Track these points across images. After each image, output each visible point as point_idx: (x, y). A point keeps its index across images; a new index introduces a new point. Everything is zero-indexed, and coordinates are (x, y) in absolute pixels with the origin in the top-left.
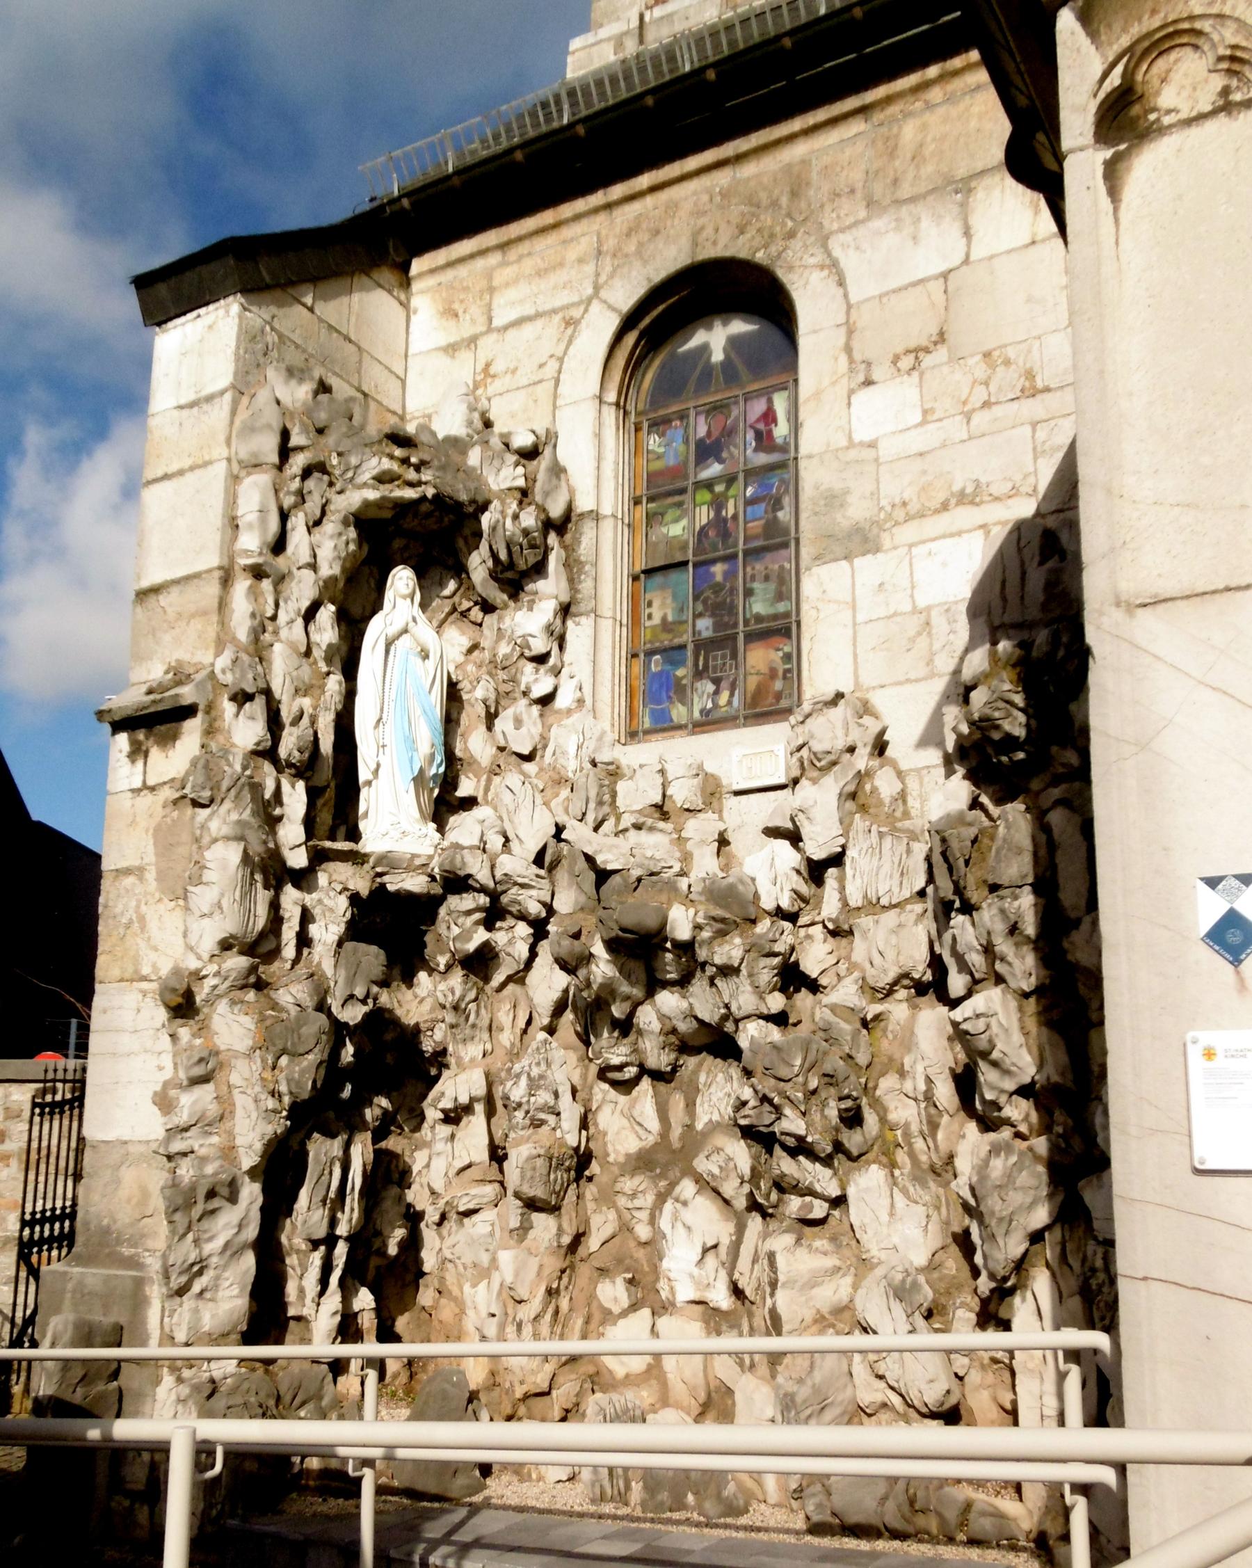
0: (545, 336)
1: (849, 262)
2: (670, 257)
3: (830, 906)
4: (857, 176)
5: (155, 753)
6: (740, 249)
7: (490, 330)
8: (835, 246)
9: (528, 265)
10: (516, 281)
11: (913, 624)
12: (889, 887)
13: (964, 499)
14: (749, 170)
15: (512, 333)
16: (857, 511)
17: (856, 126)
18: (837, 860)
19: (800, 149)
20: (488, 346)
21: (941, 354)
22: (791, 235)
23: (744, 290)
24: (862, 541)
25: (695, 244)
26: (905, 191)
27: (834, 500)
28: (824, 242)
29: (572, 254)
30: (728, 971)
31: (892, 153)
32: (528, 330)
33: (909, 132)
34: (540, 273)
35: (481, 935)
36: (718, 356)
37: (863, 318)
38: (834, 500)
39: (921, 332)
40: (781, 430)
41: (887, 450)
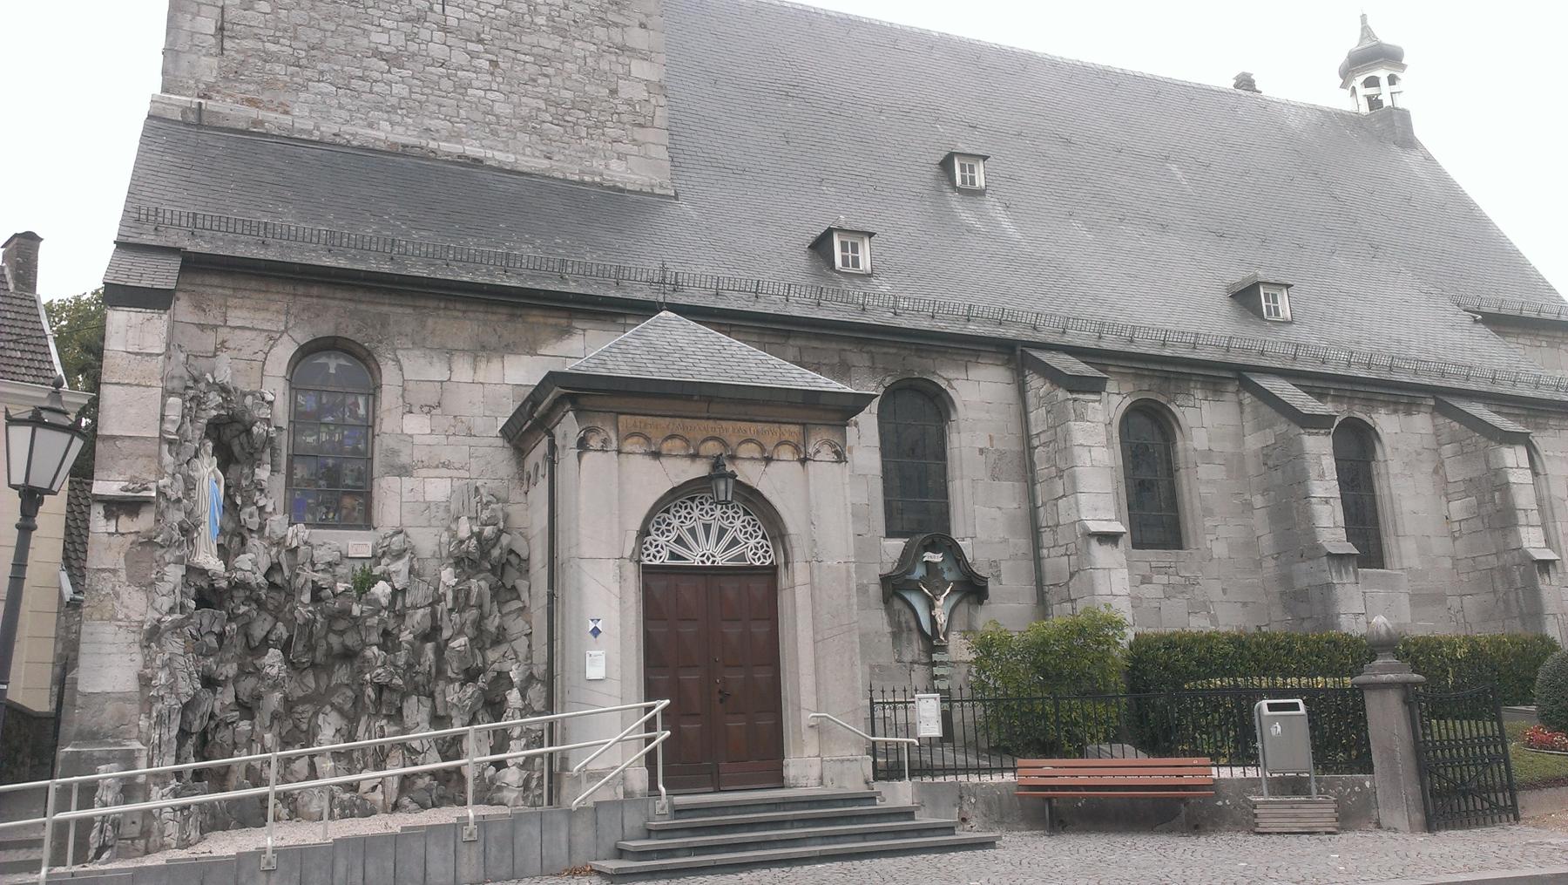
0: (260, 342)
1: (405, 363)
2: (325, 329)
3: (399, 606)
4: (409, 330)
5: (123, 519)
6: (358, 338)
7: (225, 325)
8: (399, 353)
9: (248, 302)
10: (241, 307)
11: (424, 506)
12: (420, 601)
13: (444, 465)
14: (363, 307)
15: (238, 332)
16: (404, 459)
17: (409, 311)
18: (404, 591)
19: (385, 309)
20: (223, 333)
21: (438, 411)
22: (380, 342)
23: (363, 358)
24: (404, 471)
25: (337, 328)
26: (428, 344)
27: (395, 452)
28: (395, 350)
29: (274, 307)
30: (368, 629)
31: (424, 327)
32: (248, 334)
33: (430, 322)
34: (257, 310)
35: (243, 609)
36: (332, 371)
37: (410, 386)
38: (395, 452)
39: (434, 402)
40: (362, 411)
41: (417, 440)
